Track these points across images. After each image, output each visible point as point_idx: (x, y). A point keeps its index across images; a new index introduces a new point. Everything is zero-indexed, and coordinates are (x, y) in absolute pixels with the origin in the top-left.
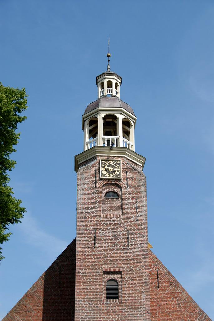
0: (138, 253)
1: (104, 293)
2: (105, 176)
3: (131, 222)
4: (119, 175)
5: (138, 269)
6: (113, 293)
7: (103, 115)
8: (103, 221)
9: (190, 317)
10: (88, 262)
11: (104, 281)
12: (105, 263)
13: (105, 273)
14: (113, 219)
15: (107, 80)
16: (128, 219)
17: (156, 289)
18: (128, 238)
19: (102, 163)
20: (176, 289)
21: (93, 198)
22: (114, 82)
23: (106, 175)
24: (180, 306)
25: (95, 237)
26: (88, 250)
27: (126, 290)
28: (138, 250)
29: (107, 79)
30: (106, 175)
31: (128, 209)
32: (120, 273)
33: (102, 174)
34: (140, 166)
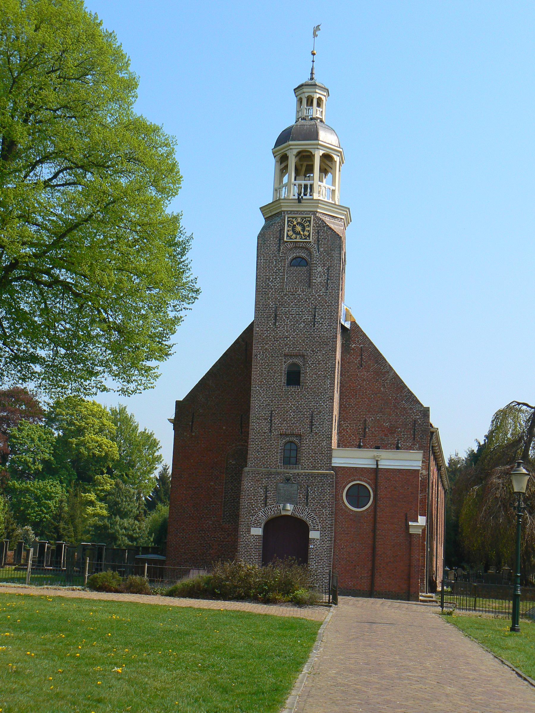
0: (325, 333)
1: (284, 379)
2: (291, 239)
3: (319, 296)
4: (309, 236)
5: (324, 353)
6: (294, 377)
8: (285, 295)
9: (396, 399)
10: (266, 344)
11: (284, 366)
13: (286, 355)
14: (298, 293)
16: (316, 292)
17: (358, 368)
18: (315, 316)
19: (288, 221)
20: (382, 368)
21: (275, 267)
23: (292, 237)
24: (384, 387)
25: (276, 316)
26: (267, 331)
27: (308, 376)
30: (292, 237)
31: (318, 280)
32: (303, 356)
33: (288, 236)
34: (341, 219)
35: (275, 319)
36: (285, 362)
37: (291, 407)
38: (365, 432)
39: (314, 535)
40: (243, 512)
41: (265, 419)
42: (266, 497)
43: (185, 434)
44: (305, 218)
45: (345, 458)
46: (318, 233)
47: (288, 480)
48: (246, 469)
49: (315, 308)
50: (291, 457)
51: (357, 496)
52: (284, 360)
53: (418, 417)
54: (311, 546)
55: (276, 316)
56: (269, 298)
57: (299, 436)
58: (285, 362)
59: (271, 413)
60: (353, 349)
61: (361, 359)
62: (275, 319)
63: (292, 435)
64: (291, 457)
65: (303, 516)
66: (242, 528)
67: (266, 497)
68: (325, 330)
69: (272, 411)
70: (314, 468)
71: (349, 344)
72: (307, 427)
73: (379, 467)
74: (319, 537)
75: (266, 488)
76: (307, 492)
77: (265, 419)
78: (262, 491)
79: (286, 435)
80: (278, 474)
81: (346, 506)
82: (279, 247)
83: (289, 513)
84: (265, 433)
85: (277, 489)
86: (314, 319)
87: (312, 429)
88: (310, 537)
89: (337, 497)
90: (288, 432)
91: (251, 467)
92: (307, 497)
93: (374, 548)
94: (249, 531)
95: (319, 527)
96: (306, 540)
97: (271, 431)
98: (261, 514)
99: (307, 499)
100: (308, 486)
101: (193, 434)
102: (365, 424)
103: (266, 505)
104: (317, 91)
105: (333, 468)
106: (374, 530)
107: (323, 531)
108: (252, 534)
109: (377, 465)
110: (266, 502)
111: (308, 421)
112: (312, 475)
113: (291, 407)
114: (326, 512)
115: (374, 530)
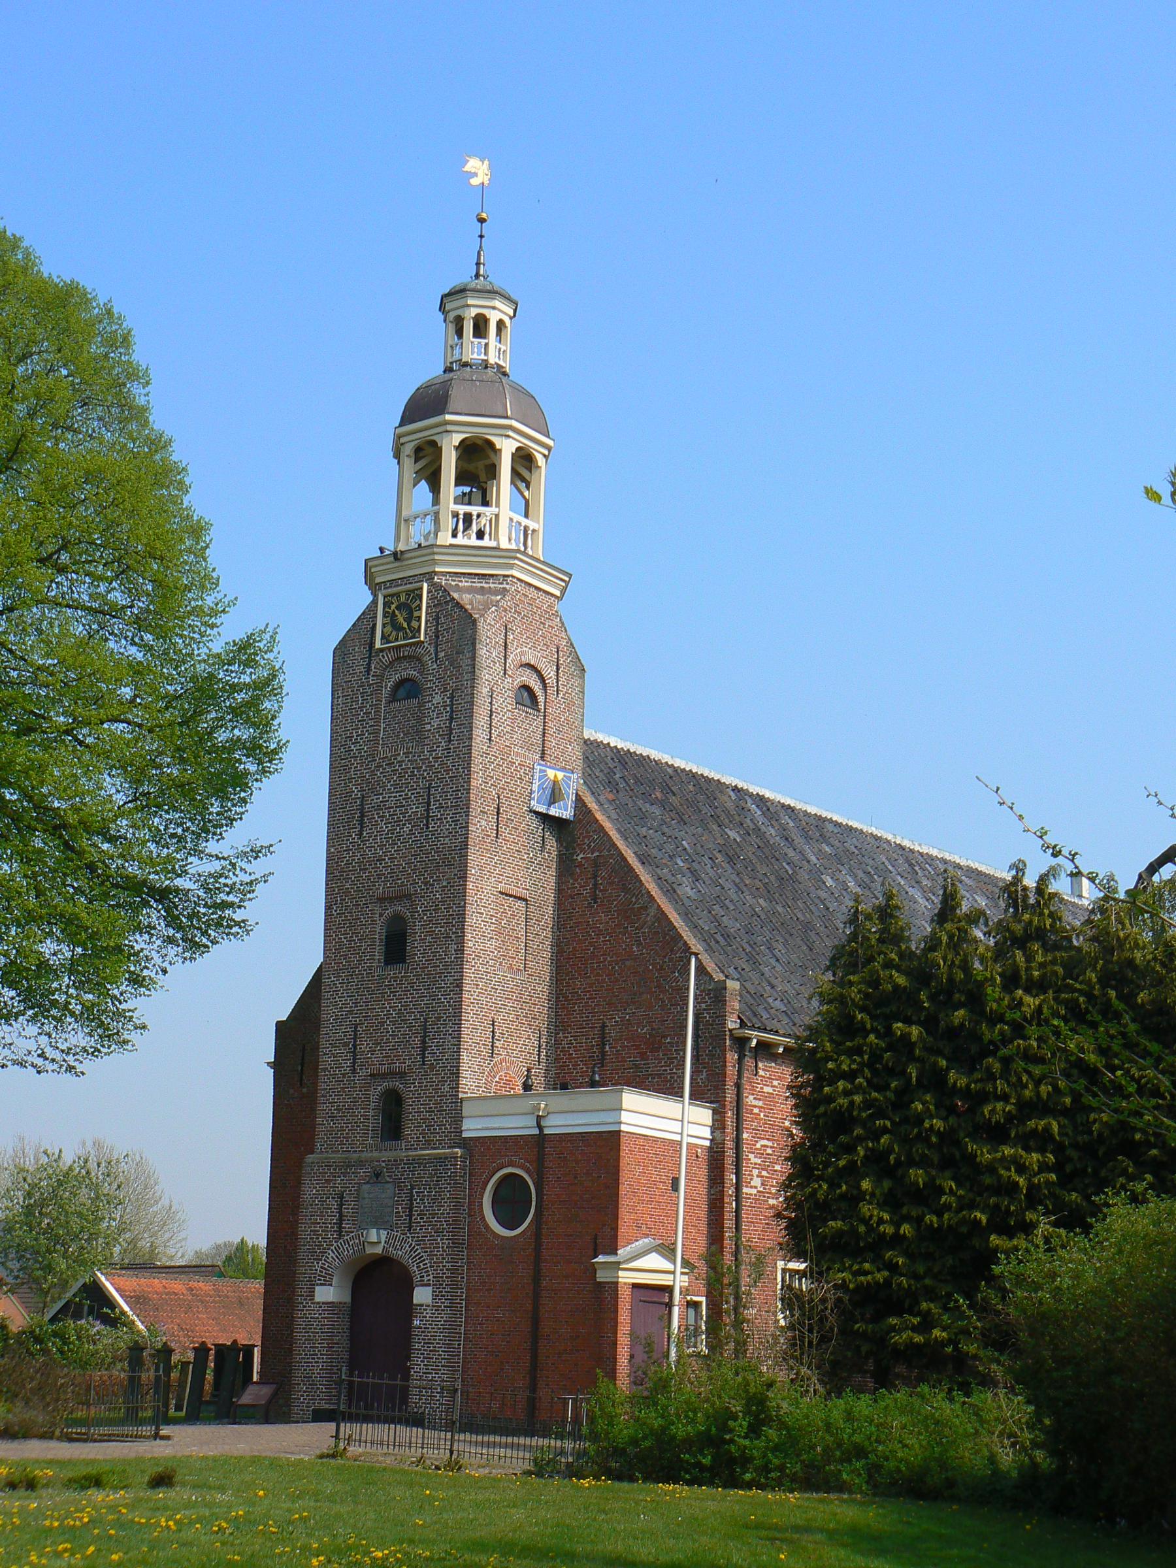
1: (379, 954)
5: (445, 884)
7: (457, 439)
9: (661, 968)
13: (381, 900)
15: (474, 312)
17: (590, 906)
18: (429, 804)
22: (493, 317)
24: (639, 944)
25: (362, 816)
29: (474, 307)
31: (435, 723)
32: (408, 896)
33: (383, 637)
35: (362, 823)
36: (381, 915)
38: (603, 1053)
39: (422, 1295)
40: (303, 1251)
41: (346, 1045)
42: (341, 1215)
43: (291, 1091)
46: (437, 618)
47: (377, 1175)
48: (310, 1158)
49: (429, 788)
50: (392, 1122)
51: (511, 1200)
52: (378, 910)
53: (703, 1006)
57: (402, 1075)
59: (355, 1031)
60: (580, 865)
61: (596, 884)
62: (362, 823)
63: (392, 1074)
64: (392, 1122)
66: (302, 1289)
67: (341, 1215)
70: (428, 1144)
71: (573, 854)
72: (416, 1053)
73: (546, 1131)
74: (429, 1301)
75: (342, 1197)
76: (411, 1200)
77: (346, 1045)
78: (334, 1204)
79: (384, 1076)
80: (361, 1163)
81: (487, 1227)
82: (369, 664)
83: (379, 1250)
84: (344, 1075)
85: (358, 1198)
86: (428, 810)
87: (424, 1057)
91: (322, 1152)
92: (411, 1211)
93: (536, 1322)
96: (408, 1308)
97: (354, 1071)
99: (410, 1216)
100: (412, 1188)
101: (305, 1090)
102: (603, 1033)
103: (340, 1236)
104: (470, 302)
105: (466, 1143)
106: (537, 1278)
107: (436, 1285)
108: (317, 1299)
112: (420, 1162)
114: (443, 1241)
115: (537, 1278)
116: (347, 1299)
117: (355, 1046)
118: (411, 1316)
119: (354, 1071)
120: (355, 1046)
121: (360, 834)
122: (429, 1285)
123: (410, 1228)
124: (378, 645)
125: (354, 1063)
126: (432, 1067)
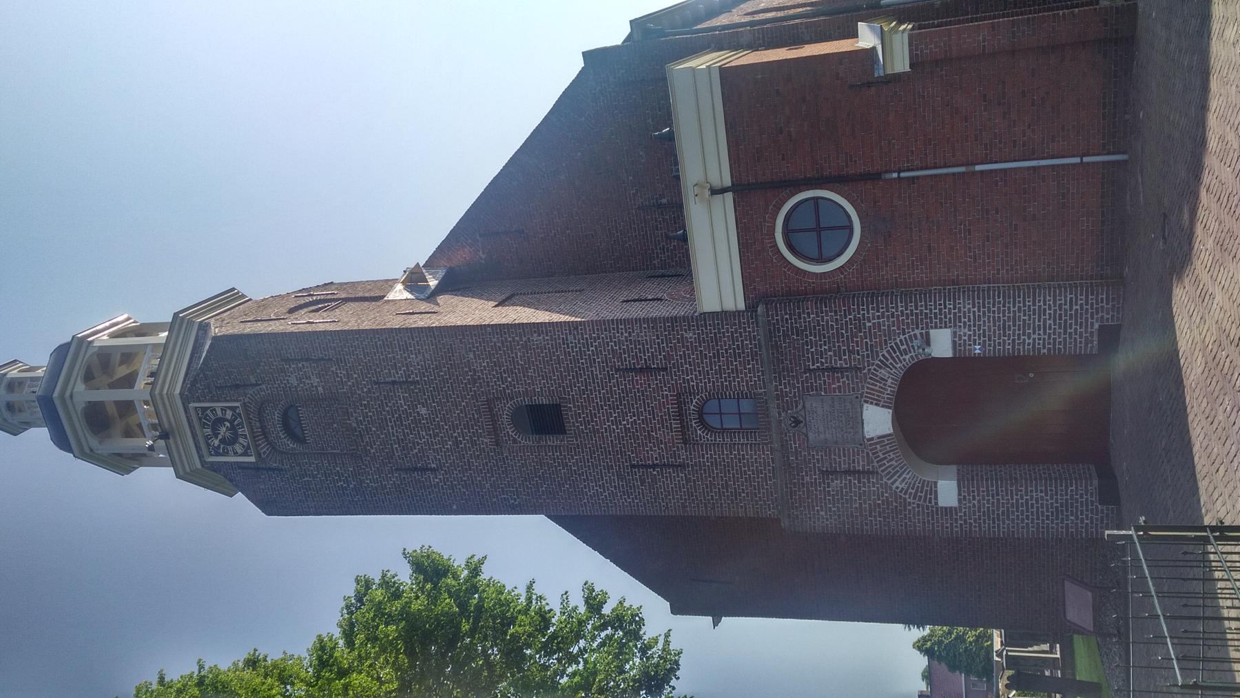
1: (552, 441)
2: (249, 447)
3: (349, 376)
4: (233, 409)
5: (472, 356)
12: (474, 443)
18: (394, 383)
19: (218, 454)
21: (314, 477)
25: (416, 469)
28: (420, 357)
33: (245, 454)
35: (424, 469)
37: (616, 422)
39: (942, 344)
44: (200, 419)
45: (718, 282)
46: (220, 388)
47: (797, 422)
49: (377, 383)
51: (817, 232)
54: (977, 350)
55: (416, 469)
56: (384, 487)
58: (515, 441)
59: (638, 466)
62: (424, 469)
63: (681, 414)
65: (890, 378)
68: (420, 357)
69: (633, 466)
73: (728, 182)
79: (684, 428)
82: (273, 470)
84: (688, 480)
86: (401, 383)
88: (949, 354)
89: (826, 292)
90: (675, 425)
94: (948, 511)
95: (917, 332)
97: (682, 466)
98: (897, 484)
99: (841, 370)
105: (751, 307)
109: (723, 191)
110: (863, 472)
111: (641, 379)
113: (616, 422)
116: (954, 468)
117: (654, 466)
118: (970, 358)
119: (682, 466)
120: (654, 466)
121: (433, 470)
122: (928, 334)
123: (858, 369)
124: (252, 459)
125: (673, 466)
126: (668, 357)
